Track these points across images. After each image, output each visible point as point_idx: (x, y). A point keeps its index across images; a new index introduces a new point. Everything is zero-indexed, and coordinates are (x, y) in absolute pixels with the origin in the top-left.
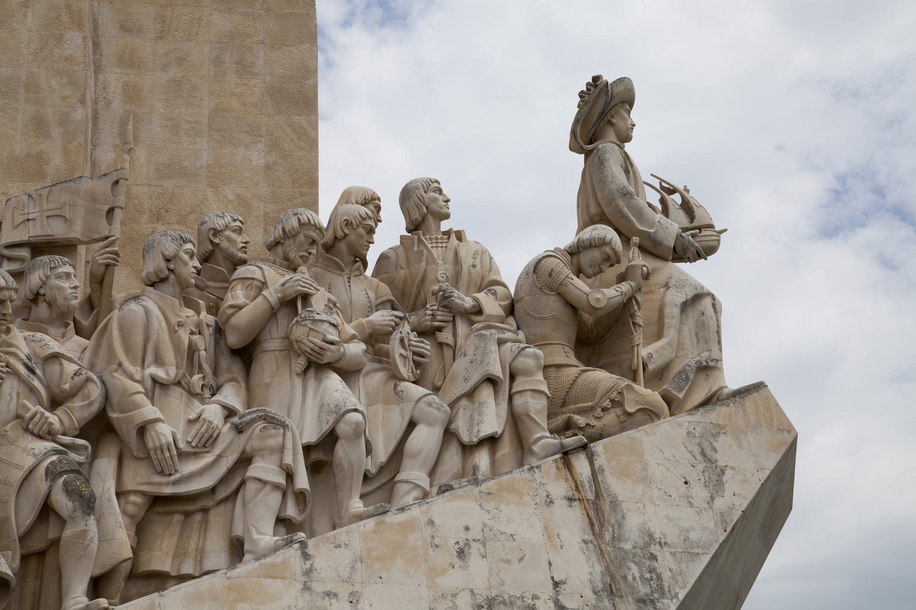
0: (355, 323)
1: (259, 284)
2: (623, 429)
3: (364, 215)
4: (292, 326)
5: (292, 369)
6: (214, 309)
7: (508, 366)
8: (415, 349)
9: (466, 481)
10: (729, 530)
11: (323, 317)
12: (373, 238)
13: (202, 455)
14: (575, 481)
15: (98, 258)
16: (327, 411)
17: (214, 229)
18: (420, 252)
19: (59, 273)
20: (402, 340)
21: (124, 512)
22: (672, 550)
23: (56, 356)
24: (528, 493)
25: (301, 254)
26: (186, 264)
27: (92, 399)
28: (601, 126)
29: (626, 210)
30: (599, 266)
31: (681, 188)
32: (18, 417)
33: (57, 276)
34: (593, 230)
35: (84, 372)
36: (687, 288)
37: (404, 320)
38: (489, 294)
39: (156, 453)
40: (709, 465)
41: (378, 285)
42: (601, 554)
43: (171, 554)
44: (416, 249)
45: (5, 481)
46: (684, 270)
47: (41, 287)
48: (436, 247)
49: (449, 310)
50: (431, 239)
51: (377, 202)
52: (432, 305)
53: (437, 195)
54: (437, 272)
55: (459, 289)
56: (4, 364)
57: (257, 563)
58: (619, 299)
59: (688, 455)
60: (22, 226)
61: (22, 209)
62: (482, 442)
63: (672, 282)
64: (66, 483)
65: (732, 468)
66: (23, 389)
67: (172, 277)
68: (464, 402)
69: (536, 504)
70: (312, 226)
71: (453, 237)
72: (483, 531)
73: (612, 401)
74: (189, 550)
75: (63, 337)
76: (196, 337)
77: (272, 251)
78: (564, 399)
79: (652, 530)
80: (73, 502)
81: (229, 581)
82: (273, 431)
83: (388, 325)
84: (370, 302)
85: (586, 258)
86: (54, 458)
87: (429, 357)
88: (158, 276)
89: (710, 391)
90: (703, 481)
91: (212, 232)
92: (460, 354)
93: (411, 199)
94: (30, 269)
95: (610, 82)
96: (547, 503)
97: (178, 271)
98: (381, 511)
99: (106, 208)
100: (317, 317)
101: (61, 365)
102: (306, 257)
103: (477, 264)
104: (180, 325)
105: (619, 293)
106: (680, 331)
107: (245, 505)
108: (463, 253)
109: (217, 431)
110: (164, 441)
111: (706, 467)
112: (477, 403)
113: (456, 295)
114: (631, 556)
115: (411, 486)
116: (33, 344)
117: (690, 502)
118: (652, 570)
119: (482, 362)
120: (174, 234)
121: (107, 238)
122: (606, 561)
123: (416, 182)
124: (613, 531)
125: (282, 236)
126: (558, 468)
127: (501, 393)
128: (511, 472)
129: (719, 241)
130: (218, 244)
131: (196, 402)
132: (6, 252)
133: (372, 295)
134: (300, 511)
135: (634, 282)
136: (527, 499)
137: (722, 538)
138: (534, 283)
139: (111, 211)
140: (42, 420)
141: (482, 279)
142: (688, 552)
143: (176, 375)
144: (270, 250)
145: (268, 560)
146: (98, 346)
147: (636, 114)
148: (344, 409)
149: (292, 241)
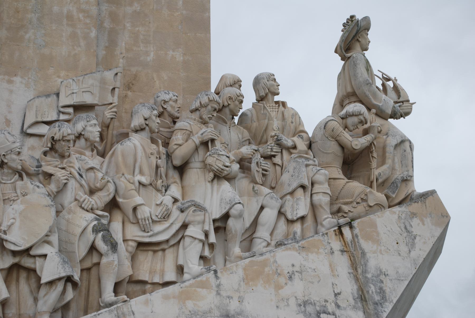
0: (233, 152)
1: (189, 132)
2: (367, 214)
3: (239, 95)
4: (207, 157)
5: (206, 178)
6: (166, 144)
7: (310, 179)
8: (263, 167)
9: (291, 240)
10: (417, 268)
11: (223, 153)
12: (242, 106)
13: (163, 222)
14: (344, 242)
15: (107, 115)
16: (225, 202)
17: (164, 100)
18: (266, 114)
19: (91, 124)
20: (257, 163)
21: (127, 250)
22: (390, 278)
23: (92, 168)
24: (322, 248)
25: (209, 116)
26: (154, 121)
27: (110, 192)
28: (353, 41)
29: (367, 93)
30: (356, 125)
31: (393, 77)
32: (76, 200)
33: (90, 125)
34: (355, 106)
35: (106, 178)
36: (397, 137)
37: (257, 152)
38: (300, 138)
39: (142, 221)
40: (409, 234)
41: (243, 130)
42: (357, 279)
43: (148, 272)
44: (262, 112)
45: (73, 233)
46: (396, 126)
47: (82, 131)
48: (273, 111)
49: (279, 146)
50: (270, 106)
51: (240, 83)
52: (271, 142)
53: (273, 83)
54: (274, 125)
55: (284, 135)
56: (69, 173)
57: (194, 280)
58: (367, 144)
59: (399, 229)
60: (70, 96)
61: (70, 87)
62: (298, 219)
63: (390, 133)
64: (103, 237)
65: (420, 236)
66: (78, 185)
67: (147, 128)
68: (288, 197)
69: (326, 253)
70: (215, 102)
71: (281, 104)
72: (301, 267)
73: (362, 199)
74: (157, 270)
75: (92, 157)
76: (159, 161)
77: (193, 113)
78: (337, 197)
79: (381, 268)
80: (107, 246)
81: (182, 289)
82: (199, 213)
83: (249, 154)
84: (240, 140)
85: (351, 121)
86: (95, 222)
87: (269, 171)
88: (140, 127)
89: (407, 193)
90: (405, 242)
91: (163, 102)
92: (285, 171)
93: (260, 84)
94: (76, 121)
95: (360, 19)
96: (331, 253)
97: (150, 125)
98: (252, 255)
99: (111, 88)
100: (221, 153)
101: (94, 173)
102: (211, 117)
103: (293, 121)
104: (152, 154)
105: (366, 141)
106: (393, 160)
107: (184, 249)
108: (286, 114)
109: (170, 210)
110: (146, 216)
111: (407, 235)
112: (296, 198)
113: (284, 139)
114: (371, 281)
115: (262, 240)
116: (81, 162)
117: (399, 253)
118: (381, 289)
119: (298, 177)
120: (149, 106)
121: (111, 104)
122: (359, 283)
123: (263, 75)
124: (363, 268)
125: (200, 106)
126: (336, 234)
127: (307, 193)
128: (313, 236)
129: (411, 109)
130: (165, 109)
131: (159, 195)
132: (62, 110)
133: (240, 136)
134: (210, 252)
135: (373, 135)
136: (321, 250)
137: (414, 272)
138: (324, 134)
139: (114, 89)
140: (89, 203)
141: (296, 129)
142: (398, 279)
143: (151, 180)
144: (192, 113)
145: (199, 279)
146: (110, 162)
147: (371, 35)
148: (234, 203)
149: (204, 109)
